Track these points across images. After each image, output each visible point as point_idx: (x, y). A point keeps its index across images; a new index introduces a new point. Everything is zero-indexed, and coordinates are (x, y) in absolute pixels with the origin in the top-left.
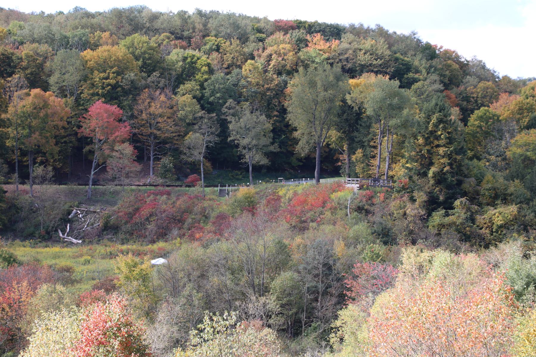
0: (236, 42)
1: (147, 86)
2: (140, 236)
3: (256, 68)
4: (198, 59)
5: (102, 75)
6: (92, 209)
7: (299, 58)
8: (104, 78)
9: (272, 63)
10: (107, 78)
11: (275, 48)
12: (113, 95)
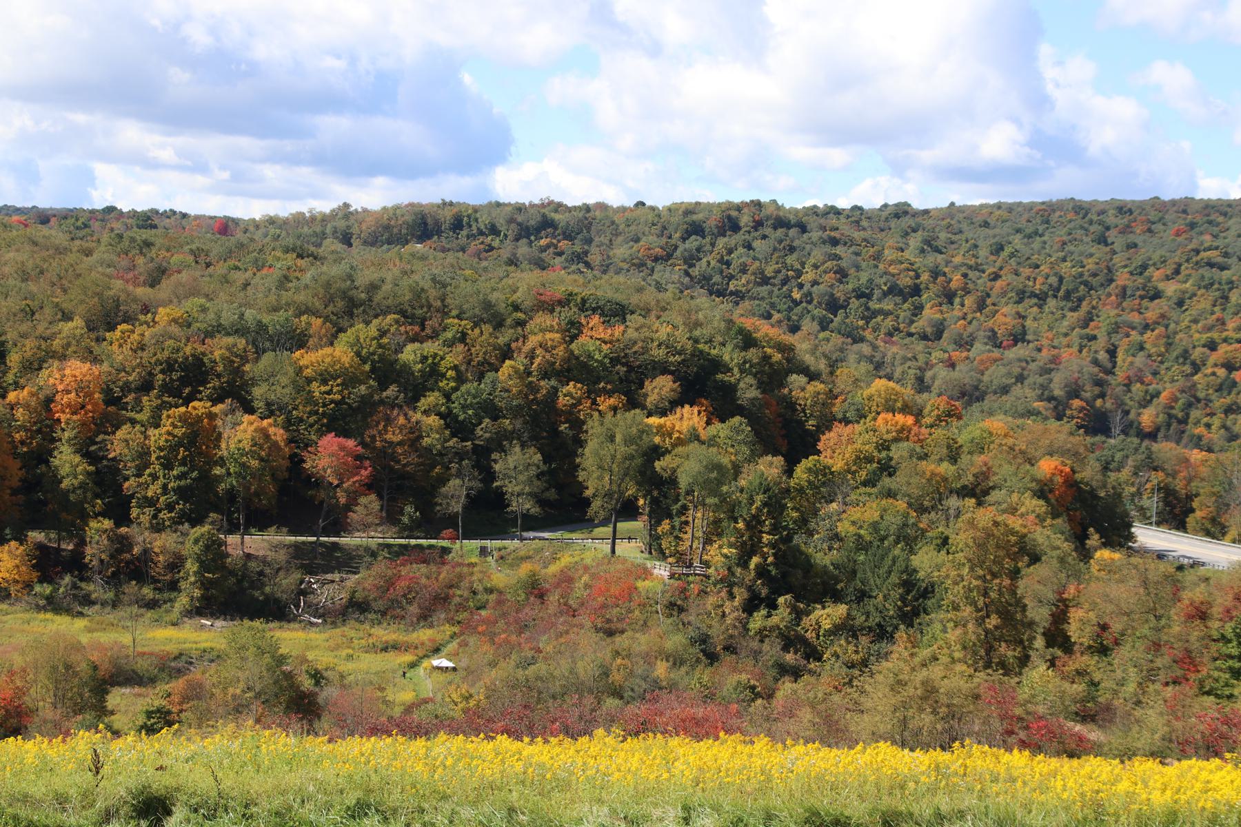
0: (487, 328)
1: (382, 402)
2: (394, 617)
3: (517, 371)
4: (442, 359)
5: (323, 389)
6: (329, 576)
7: (572, 352)
8: (326, 393)
9: (537, 361)
10: (328, 393)
11: (539, 337)
12: (342, 420)
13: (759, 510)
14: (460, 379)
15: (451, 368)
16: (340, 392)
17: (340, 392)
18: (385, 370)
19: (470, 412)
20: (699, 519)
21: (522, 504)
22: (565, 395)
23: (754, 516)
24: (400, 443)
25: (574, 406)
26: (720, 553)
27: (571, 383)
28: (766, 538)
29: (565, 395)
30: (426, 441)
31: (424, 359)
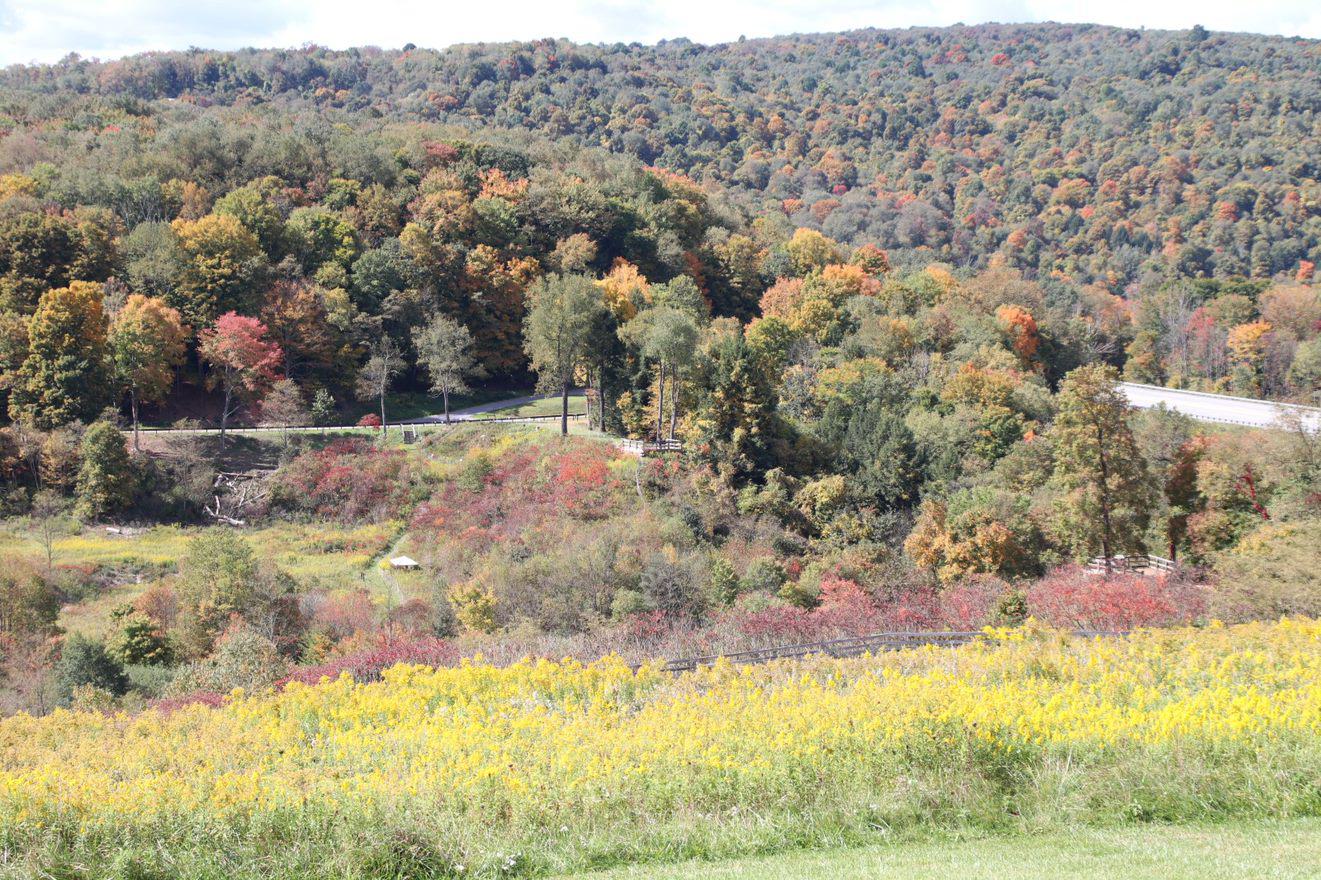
1: (275, 276)
4: (336, 224)
5: (210, 262)
8: (213, 267)
13: (740, 376)
14: (358, 247)
15: (347, 234)
16: (229, 266)
17: (229, 266)
18: (275, 241)
19: (375, 282)
20: (663, 390)
21: (444, 384)
22: (474, 260)
23: (733, 384)
24: (302, 321)
25: (484, 271)
26: (696, 427)
27: (480, 246)
28: (748, 407)
29: (474, 260)
30: (331, 317)
31: (316, 225)
